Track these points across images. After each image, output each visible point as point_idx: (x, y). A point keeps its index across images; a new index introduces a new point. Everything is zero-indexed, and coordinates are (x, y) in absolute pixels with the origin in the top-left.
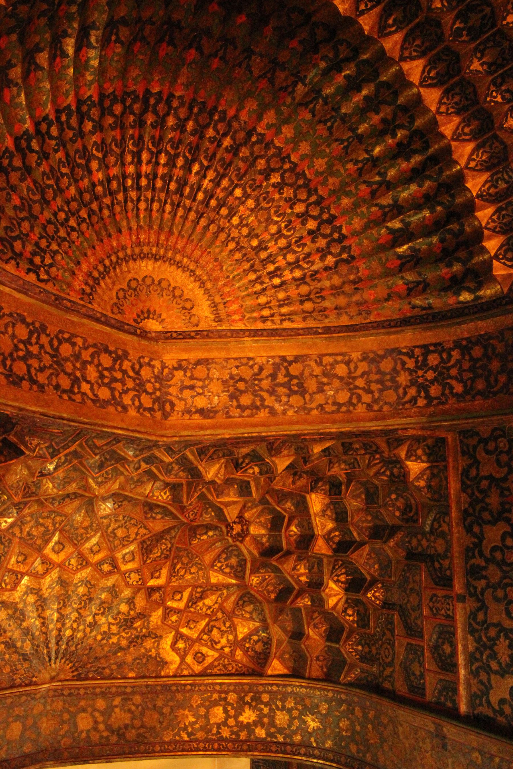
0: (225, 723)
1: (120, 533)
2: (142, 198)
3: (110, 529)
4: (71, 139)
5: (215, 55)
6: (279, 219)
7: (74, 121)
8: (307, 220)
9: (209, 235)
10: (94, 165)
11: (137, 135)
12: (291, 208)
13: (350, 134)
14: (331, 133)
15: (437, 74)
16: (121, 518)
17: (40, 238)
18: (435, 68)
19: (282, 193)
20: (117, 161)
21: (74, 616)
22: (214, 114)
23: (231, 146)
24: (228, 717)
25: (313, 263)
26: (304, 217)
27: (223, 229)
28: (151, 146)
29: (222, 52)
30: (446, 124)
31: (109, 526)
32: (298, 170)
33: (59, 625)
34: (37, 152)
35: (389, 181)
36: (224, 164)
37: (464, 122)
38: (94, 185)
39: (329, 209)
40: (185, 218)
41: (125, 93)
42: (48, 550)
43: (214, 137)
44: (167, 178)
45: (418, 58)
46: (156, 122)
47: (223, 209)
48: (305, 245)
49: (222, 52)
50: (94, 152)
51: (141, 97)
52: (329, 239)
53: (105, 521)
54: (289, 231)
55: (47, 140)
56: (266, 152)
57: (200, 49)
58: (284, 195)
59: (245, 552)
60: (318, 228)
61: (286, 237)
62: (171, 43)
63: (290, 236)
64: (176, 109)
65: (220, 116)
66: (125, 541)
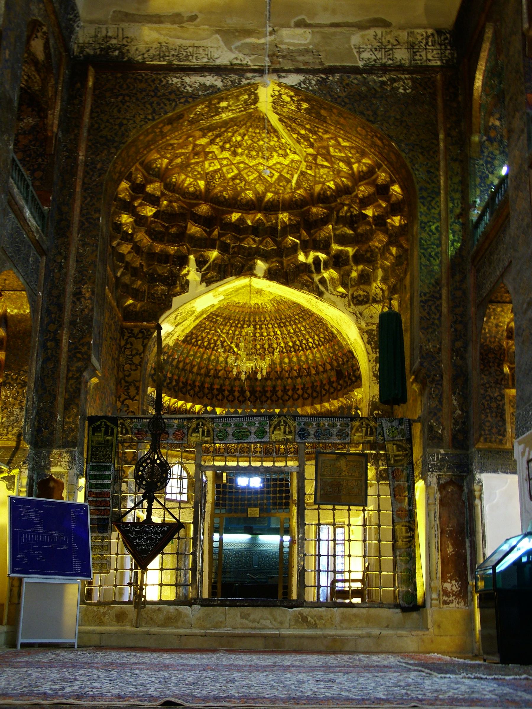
0: (161, 128)
1: (238, 181)
3: (243, 183)
7: (304, 346)
10: (292, 331)
16: (239, 189)
21: (255, 140)
24: (161, 132)
26: (203, 339)
31: (245, 185)
33: (264, 135)
42: (276, 175)
53: (247, 187)
59: (166, 192)
62: (277, 372)
66: (234, 178)
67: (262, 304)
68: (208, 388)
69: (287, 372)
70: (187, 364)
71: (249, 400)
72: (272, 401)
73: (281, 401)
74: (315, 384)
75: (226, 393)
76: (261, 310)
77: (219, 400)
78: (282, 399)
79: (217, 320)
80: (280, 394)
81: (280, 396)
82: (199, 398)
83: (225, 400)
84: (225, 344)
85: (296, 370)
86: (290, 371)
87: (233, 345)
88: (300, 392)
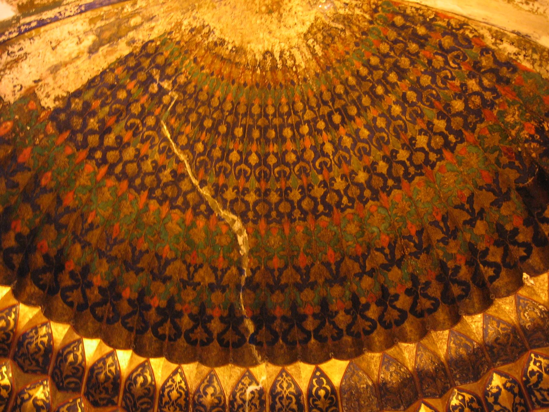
2: (300, 114)
4: (397, 152)
5: (281, 271)
6: (146, 133)
8: (117, 143)
9: (218, 93)
11: (325, 171)
12: (138, 150)
13: (113, 253)
14: (131, 244)
15: (66, 360)
17: (418, 53)
18: (71, 363)
19: (152, 162)
20: (340, 143)
22: (254, 217)
23: (223, 192)
25: (96, 97)
26: (121, 145)
27: (203, 104)
28: (307, 166)
29: (276, 276)
30: (36, 316)
32: (145, 194)
34: (435, 134)
35: (51, 224)
36: (224, 172)
37: (12, 330)
38: (359, 114)
39: (99, 165)
40: (249, 106)
41: (352, 207)
43: (244, 194)
44: (281, 139)
45: (95, 365)
46: (310, 191)
47: (210, 125)
48: (110, 114)
49: (276, 276)
50: (367, 146)
51: (335, 208)
52: (86, 130)
54: (132, 125)
55: (425, 146)
56: (185, 198)
57: (297, 269)
58: (149, 162)
60: (102, 139)
61: (133, 116)
62: (327, 265)
63: (129, 119)
64: (293, 208)
65: (247, 216)
67: (282, 53)
68: (130, 301)
69: (356, 259)
70: (68, 210)
71: (253, 340)
72: (321, 339)
73: (347, 339)
74: (450, 264)
75: (186, 322)
76: (280, 76)
77: (162, 338)
78: (349, 333)
79: (162, 91)
80: (342, 319)
81: (343, 326)
82: (99, 319)
83: (182, 342)
84: (185, 186)
85: (381, 250)
86: (365, 257)
87: (205, 192)
88: (403, 302)
